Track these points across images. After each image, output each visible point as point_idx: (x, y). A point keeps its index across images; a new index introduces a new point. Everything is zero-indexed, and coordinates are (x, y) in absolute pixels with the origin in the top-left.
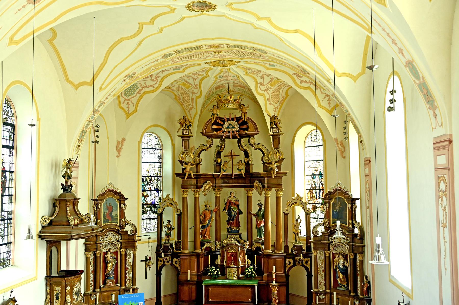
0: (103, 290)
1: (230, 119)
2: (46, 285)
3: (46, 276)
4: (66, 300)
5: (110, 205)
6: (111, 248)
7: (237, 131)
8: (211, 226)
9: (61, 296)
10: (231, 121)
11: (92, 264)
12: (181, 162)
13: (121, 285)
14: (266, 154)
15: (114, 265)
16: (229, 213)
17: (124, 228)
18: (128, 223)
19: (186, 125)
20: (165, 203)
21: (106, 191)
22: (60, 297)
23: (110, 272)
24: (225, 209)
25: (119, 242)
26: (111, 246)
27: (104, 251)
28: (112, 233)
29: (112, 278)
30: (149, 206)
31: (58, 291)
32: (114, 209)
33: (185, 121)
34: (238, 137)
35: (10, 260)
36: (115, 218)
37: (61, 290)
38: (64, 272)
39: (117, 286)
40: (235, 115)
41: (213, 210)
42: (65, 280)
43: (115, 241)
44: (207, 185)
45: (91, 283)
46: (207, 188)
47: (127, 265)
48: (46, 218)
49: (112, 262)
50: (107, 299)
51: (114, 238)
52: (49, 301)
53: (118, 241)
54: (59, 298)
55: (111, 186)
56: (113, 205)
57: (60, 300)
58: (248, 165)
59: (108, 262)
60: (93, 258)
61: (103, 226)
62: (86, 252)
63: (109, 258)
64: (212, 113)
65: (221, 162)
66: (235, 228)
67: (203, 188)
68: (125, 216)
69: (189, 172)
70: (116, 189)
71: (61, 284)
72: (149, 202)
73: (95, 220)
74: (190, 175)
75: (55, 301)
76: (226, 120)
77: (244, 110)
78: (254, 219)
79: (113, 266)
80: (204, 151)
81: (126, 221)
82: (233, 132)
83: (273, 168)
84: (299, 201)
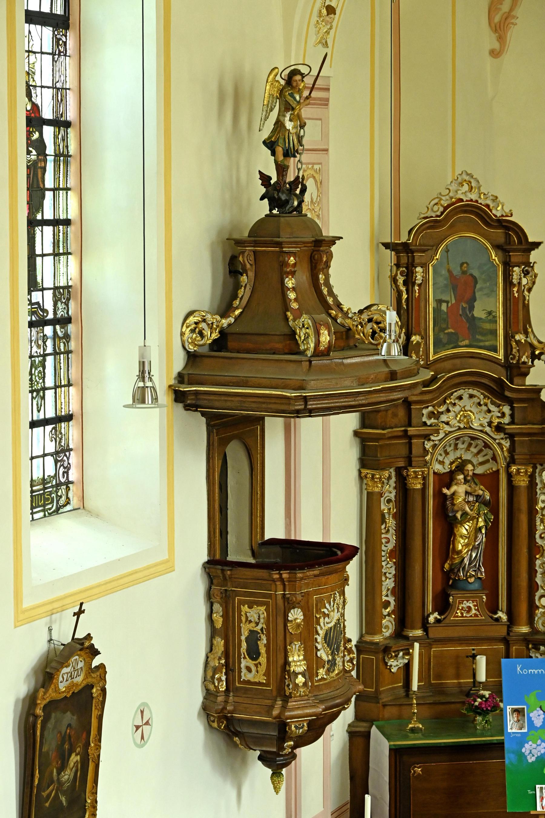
0: (434, 633)
2: (209, 597)
3: (205, 558)
4: (286, 663)
5: (464, 273)
6: (467, 456)
9: (267, 646)
11: (391, 522)
13: (512, 620)
15: (483, 531)
17: (526, 374)
18: (541, 354)
21: (445, 208)
22: (263, 650)
23: (466, 561)
25: (502, 435)
26: (468, 449)
27: (438, 467)
28: (475, 392)
29: (472, 587)
31: (257, 624)
32: (481, 289)
35: (68, 489)
36: (487, 326)
37: (267, 622)
38: (277, 549)
39: (498, 620)
42: (281, 579)
43: (488, 429)
45: (387, 604)
47: (537, 536)
48: (204, 321)
49: (473, 518)
50: (451, 671)
51: (483, 414)
52: (223, 661)
53: (499, 428)
54: (258, 654)
55: (466, 187)
56: (476, 273)
57: (263, 659)
59: (459, 515)
60: (392, 496)
61: (436, 361)
62: (364, 471)
63: (459, 500)
68: (527, 320)
70: (489, 202)
71: (269, 596)
73: (403, 335)
75: (243, 664)
79: (480, 536)
81: (535, 343)
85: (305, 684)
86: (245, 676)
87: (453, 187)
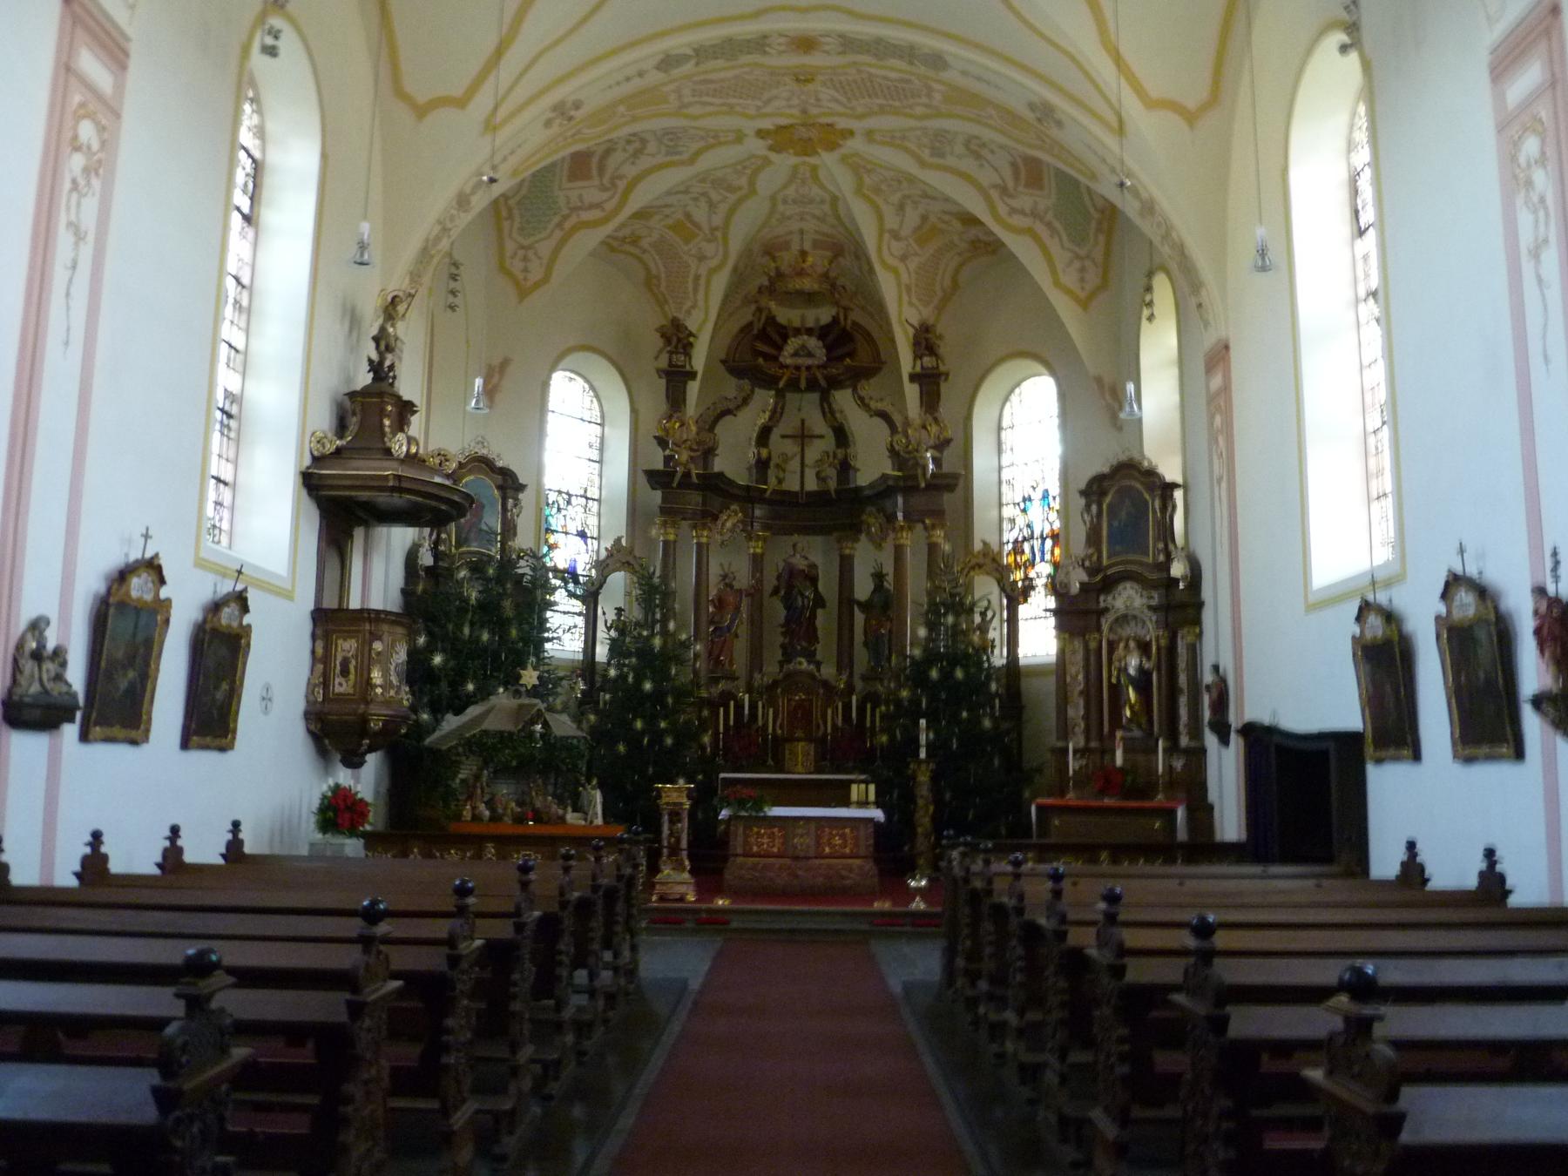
1: (803, 331)
4: (370, 678)
7: (819, 367)
8: (737, 636)
9: (356, 668)
10: (805, 337)
12: (662, 442)
14: (900, 429)
16: (789, 604)
19: (679, 340)
20: (608, 561)
24: (776, 591)
30: (560, 575)
33: (678, 330)
34: (823, 383)
40: (817, 320)
41: (746, 590)
44: (729, 516)
46: (729, 524)
58: (845, 468)
64: (753, 307)
65: (769, 458)
66: (804, 644)
67: (719, 522)
69: (685, 465)
71: (358, 631)
72: (562, 565)
74: (687, 475)
75: (337, 681)
76: (791, 333)
77: (845, 302)
78: (859, 617)
80: (729, 418)
82: (808, 368)
83: (921, 462)
84: (988, 561)
85: (382, 694)
86: (338, 689)
87: (473, 444)
